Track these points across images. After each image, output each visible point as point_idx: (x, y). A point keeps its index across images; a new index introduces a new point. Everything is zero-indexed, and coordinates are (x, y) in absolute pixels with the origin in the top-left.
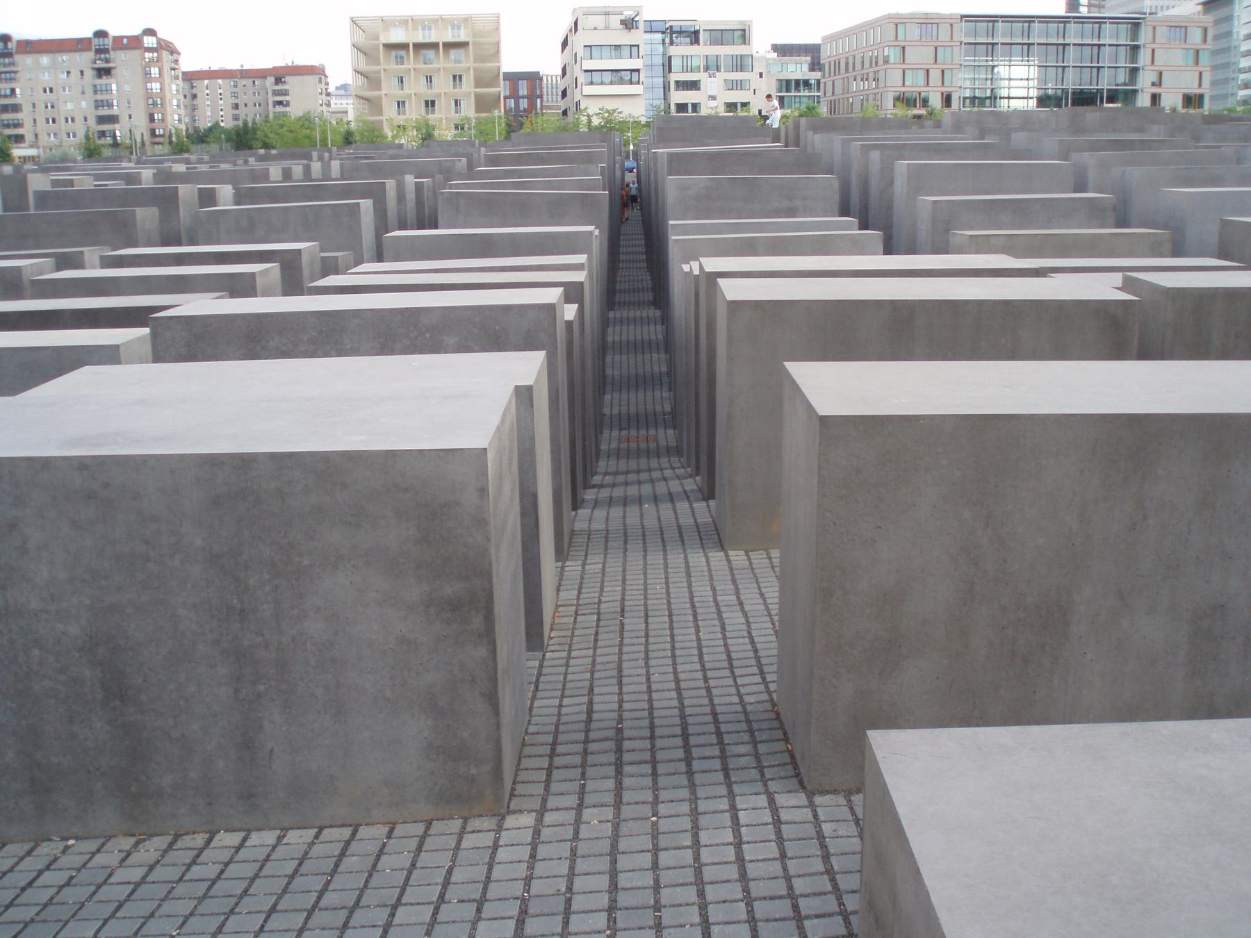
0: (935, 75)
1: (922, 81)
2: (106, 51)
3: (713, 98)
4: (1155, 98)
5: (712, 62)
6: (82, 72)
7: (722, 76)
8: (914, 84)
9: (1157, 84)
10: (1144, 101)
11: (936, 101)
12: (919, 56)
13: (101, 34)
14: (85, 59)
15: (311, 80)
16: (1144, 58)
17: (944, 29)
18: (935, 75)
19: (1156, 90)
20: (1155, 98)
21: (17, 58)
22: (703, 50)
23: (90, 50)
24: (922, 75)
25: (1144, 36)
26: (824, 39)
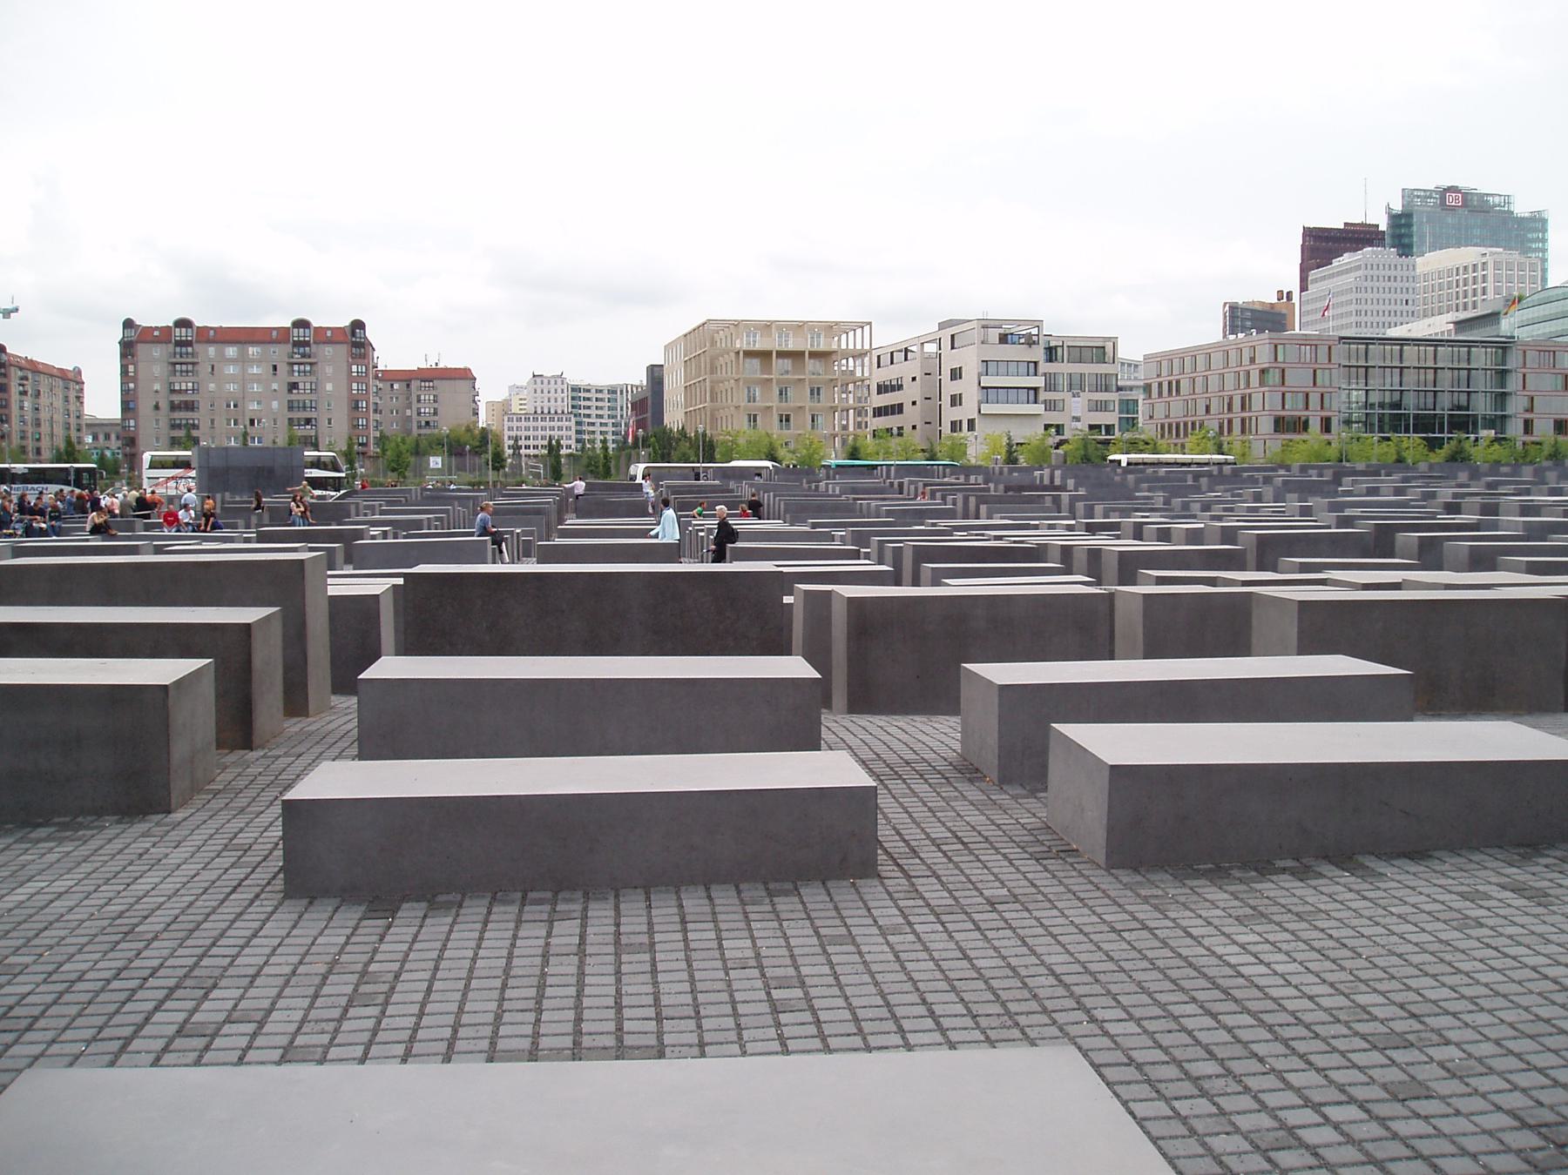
0: (1314, 400)
1: (1301, 405)
2: (189, 344)
3: (1077, 419)
4: (1528, 426)
5: (1076, 380)
6: (275, 368)
7: (1086, 396)
8: (1293, 409)
9: (1531, 409)
10: (1515, 429)
11: (1315, 425)
12: (1298, 379)
13: (183, 323)
14: (279, 353)
15: (463, 385)
16: (1513, 384)
17: (1323, 351)
18: (1314, 400)
19: (1528, 416)
20: (1528, 426)
21: (198, 347)
22: (1062, 368)
23: (287, 342)
24: (1301, 397)
25: (1513, 362)
26: (1146, 357)
